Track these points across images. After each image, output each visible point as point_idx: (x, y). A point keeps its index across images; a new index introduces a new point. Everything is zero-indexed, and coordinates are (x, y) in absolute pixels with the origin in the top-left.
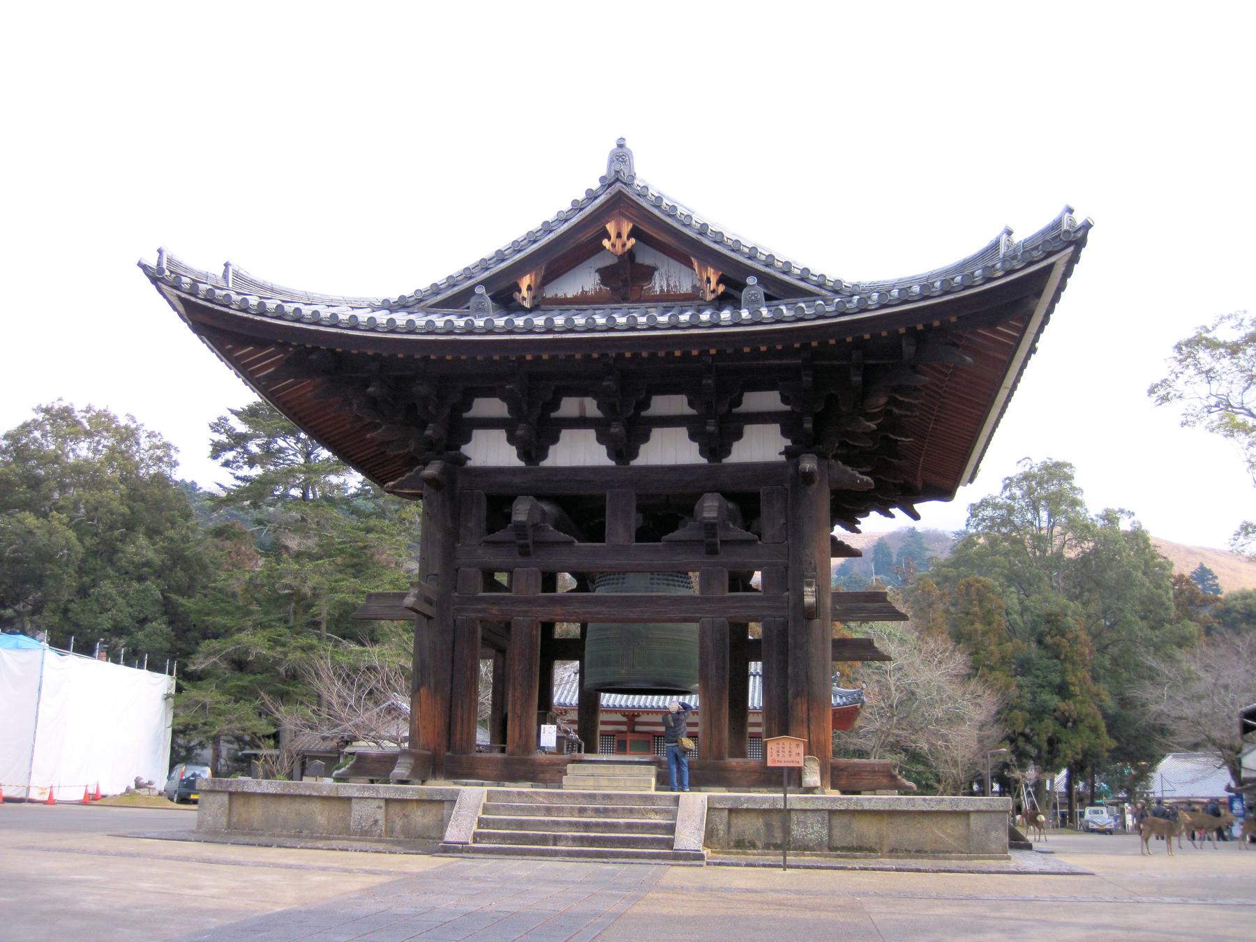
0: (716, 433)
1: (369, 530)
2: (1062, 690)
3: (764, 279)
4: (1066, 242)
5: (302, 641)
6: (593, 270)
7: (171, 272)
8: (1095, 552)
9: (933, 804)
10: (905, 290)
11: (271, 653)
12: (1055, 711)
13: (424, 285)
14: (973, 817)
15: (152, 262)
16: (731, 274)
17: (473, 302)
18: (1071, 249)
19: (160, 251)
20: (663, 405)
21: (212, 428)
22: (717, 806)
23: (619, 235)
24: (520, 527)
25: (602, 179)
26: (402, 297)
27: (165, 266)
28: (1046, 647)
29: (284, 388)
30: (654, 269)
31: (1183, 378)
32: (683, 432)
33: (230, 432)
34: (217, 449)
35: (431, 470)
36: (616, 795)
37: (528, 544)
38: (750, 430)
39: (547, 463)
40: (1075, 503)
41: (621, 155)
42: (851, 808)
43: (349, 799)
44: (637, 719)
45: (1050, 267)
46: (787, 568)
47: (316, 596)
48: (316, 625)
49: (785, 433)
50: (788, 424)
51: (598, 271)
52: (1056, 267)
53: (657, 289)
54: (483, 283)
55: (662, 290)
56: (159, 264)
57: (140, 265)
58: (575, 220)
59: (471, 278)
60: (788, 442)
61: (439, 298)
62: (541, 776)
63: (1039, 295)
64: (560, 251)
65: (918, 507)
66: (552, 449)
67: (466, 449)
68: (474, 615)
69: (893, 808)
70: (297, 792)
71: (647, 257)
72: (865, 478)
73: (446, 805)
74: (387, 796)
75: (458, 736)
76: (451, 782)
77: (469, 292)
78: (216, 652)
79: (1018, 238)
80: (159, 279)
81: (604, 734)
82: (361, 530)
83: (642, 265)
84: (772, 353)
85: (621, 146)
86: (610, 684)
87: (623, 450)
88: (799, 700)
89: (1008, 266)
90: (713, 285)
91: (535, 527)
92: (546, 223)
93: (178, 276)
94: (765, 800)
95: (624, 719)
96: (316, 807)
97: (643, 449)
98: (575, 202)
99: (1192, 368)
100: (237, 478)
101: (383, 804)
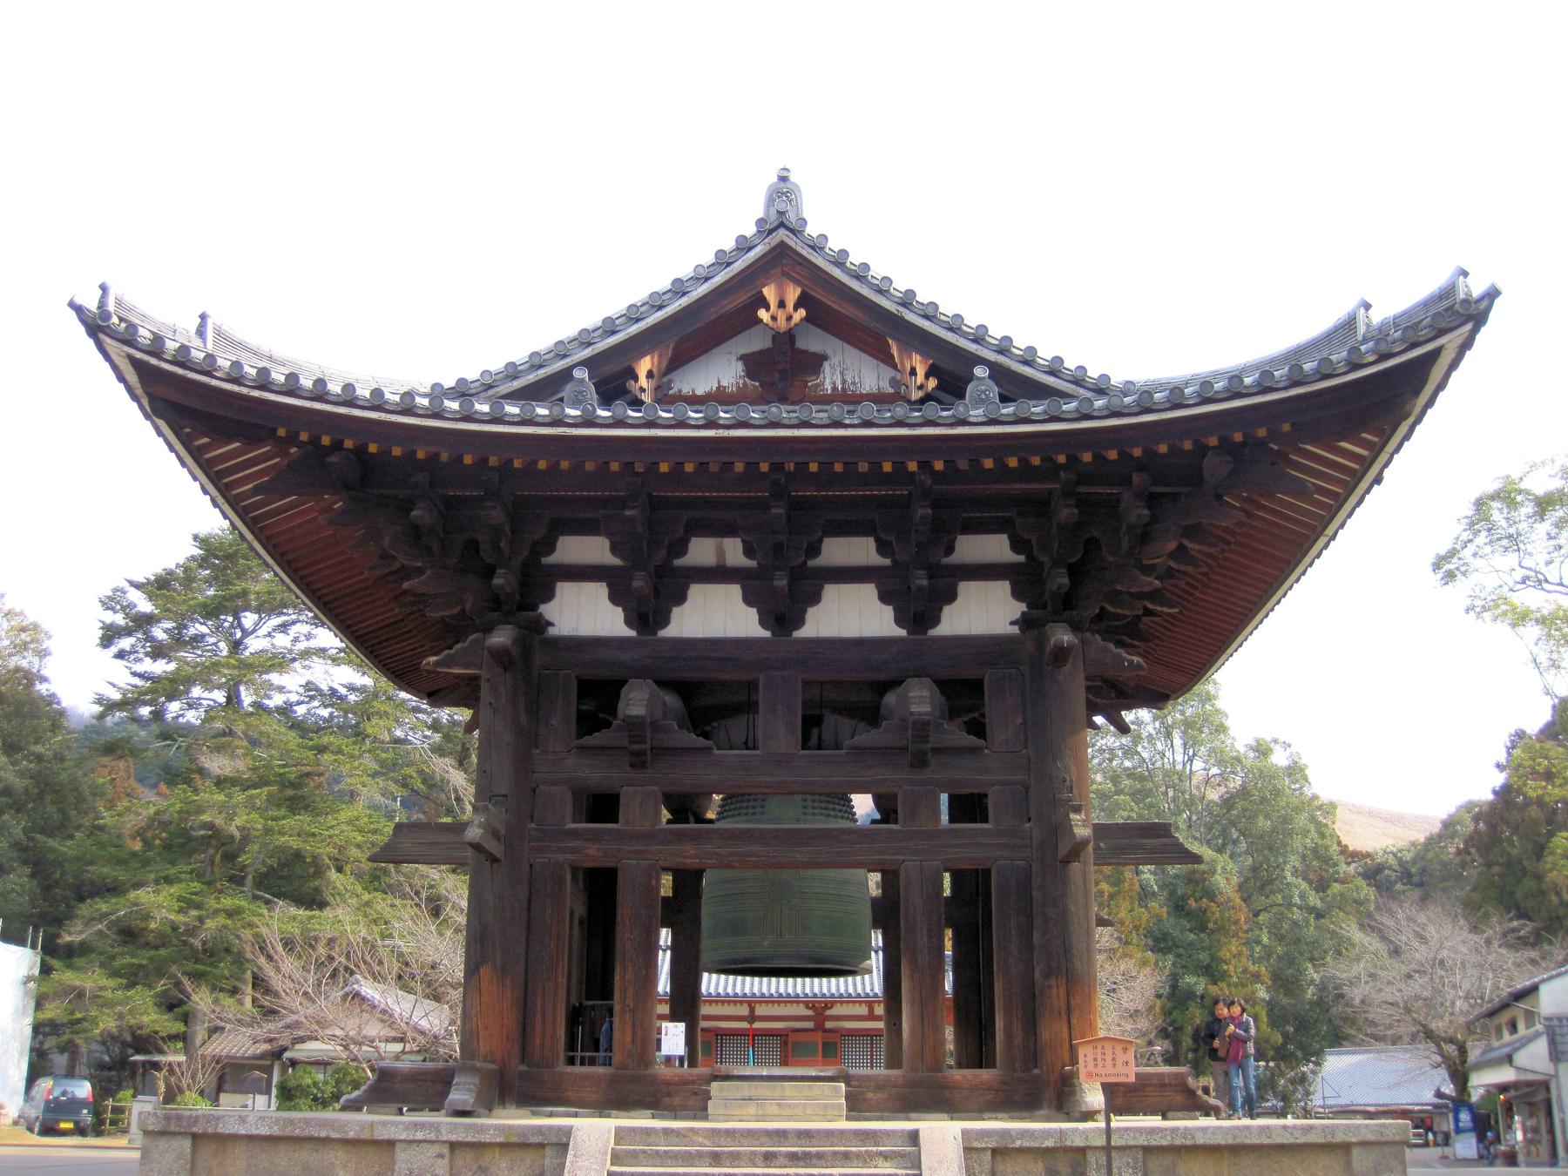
0: (918, 591)
1: (321, 750)
2: (1212, 972)
3: (999, 374)
4: (1456, 317)
5: (227, 902)
6: (734, 358)
7: (121, 319)
8: (1244, 792)
9: (1297, 1134)
10: (1235, 377)
11: (181, 918)
12: (1202, 997)
13: (496, 365)
14: (1355, 1152)
15: (91, 303)
16: (946, 364)
17: (568, 391)
18: (1469, 326)
19: (104, 288)
20: (841, 550)
21: (103, 603)
22: (976, 1144)
23: (782, 304)
24: (634, 725)
25: (760, 222)
26: (461, 381)
27: (111, 307)
28: (1189, 915)
29: (278, 511)
30: (824, 358)
31: (1471, 548)
32: (869, 591)
33: (127, 609)
34: (109, 635)
35: (501, 637)
36: (818, 1131)
37: (643, 750)
38: (967, 589)
39: (670, 632)
40: (1221, 729)
41: (783, 189)
42: (1178, 1142)
43: (391, 1144)
44: (828, 1012)
45: (1434, 355)
46: (1027, 788)
47: (246, 839)
48: (237, 880)
49: (1017, 594)
50: (1024, 581)
51: (743, 358)
52: (1444, 353)
53: (828, 387)
54: (584, 363)
55: (835, 388)
56: (102, 304)
57: (72, 305)
58: (718, 280)
59: (565, 356)
60: (1023, 607)
61: (517, 384)
62: (666, 1100)
63: (1417, 393)
64: (698, 322)
65: (1128, 716)
66: (676, 612)
67: (548, 610)
68: (561, 857)
69: (1239, 1141)
70: (306, 1133)
71: (814, 341)
72: (1136, 659)
73: (549, 1151)
74: (453, 1138)
75: (538, 1041)
76: (525, 1111)
77: (565, 376)
78: (104, 916)
79: (1378, 316)
80: (102, 329)
81: (703, 1030)
82: (311, 749)
83: (805, 352)
84: (1026, 472)
85: (783, 179)
86: (747, 961)
87: (782, 613)
88: (1053, 981)
89: (1383, 348)
90: (920, 378)
91: (656, 727)
92: (677, 281)
93: (132, 327)
94: (1047, 1134)
95: (810, 1013)
96: (336, 1156)
97: (812, 614)
98: (720, 253)
99: (1484, 534)
100: (134, 674)
101: (445, 1150)
